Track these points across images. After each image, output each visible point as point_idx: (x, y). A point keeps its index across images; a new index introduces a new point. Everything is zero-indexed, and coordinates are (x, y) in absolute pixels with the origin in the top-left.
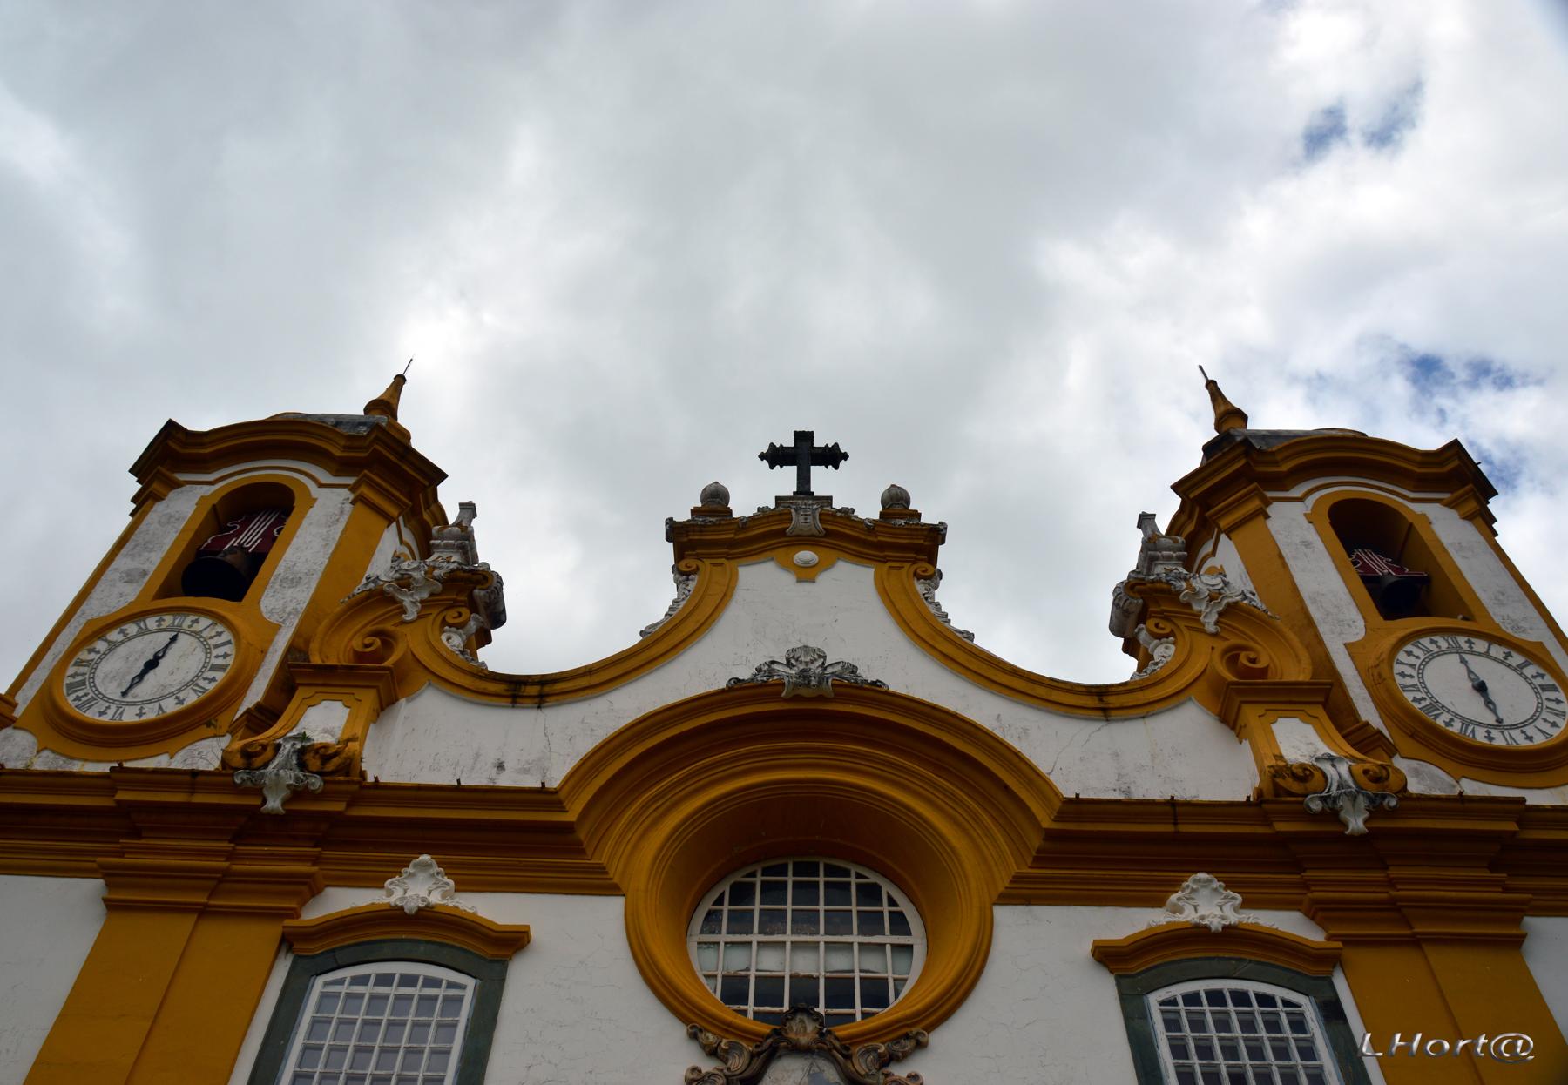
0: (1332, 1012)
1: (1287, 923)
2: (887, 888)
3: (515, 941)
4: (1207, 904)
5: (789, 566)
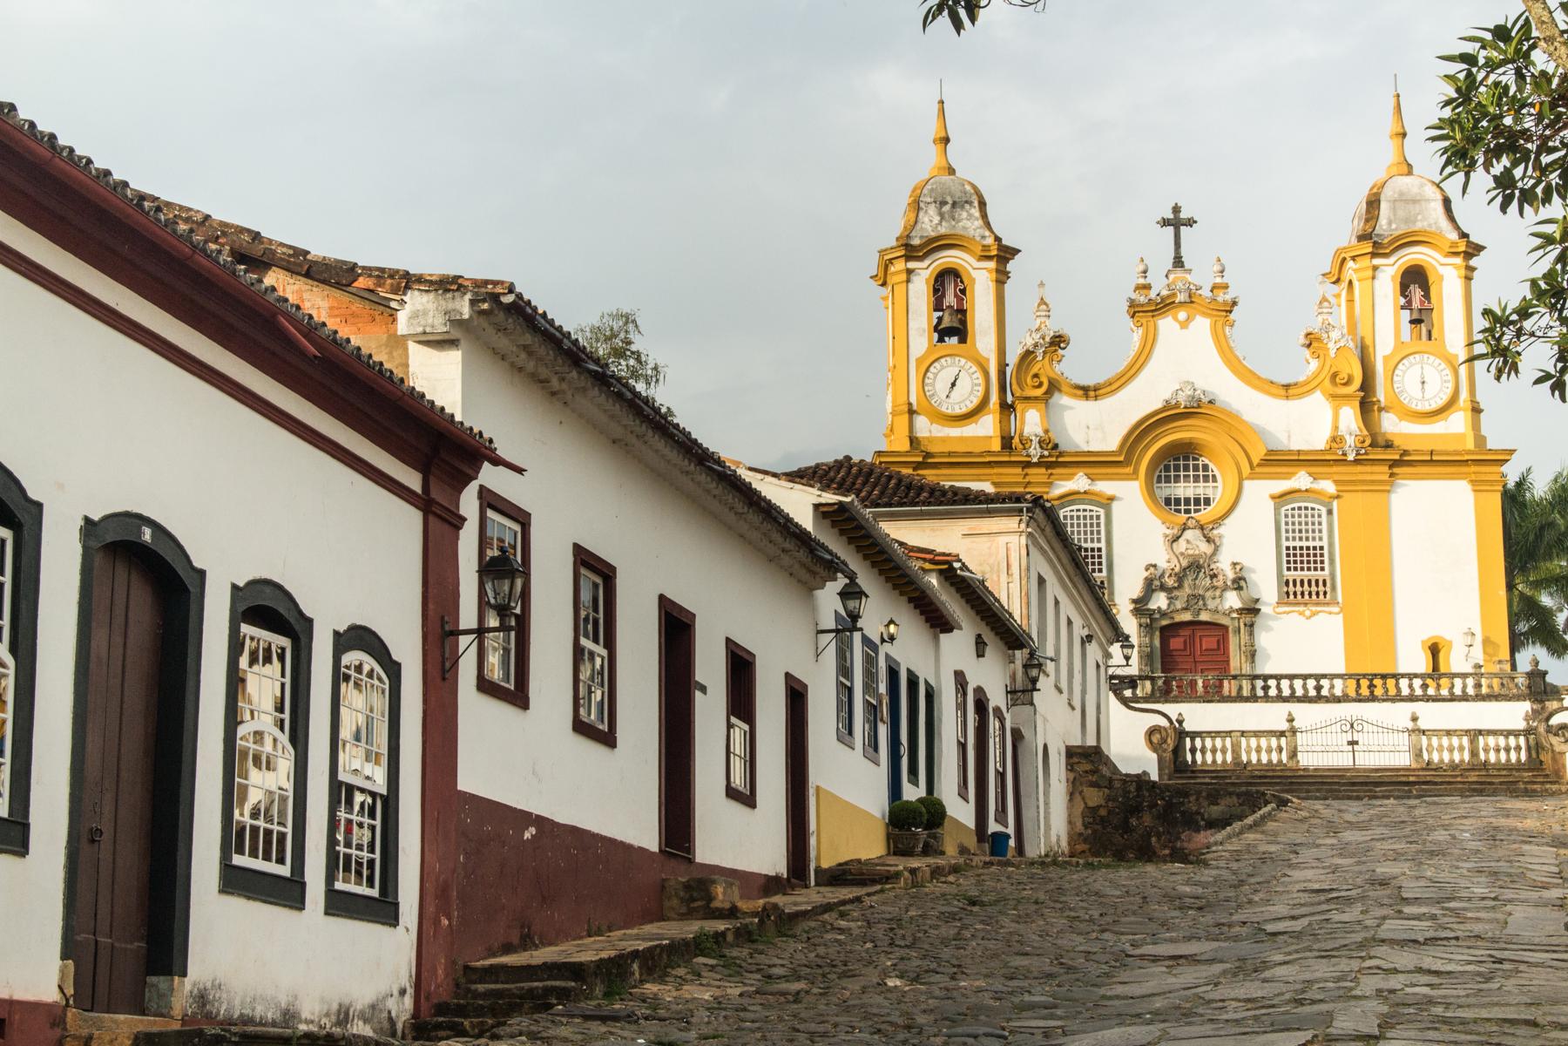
0: (1330, 512)
1: (1328, 487)
2: (1211, 466)
3: (1112, 499)
4: (1301, 480)
5: (1176, 319)
